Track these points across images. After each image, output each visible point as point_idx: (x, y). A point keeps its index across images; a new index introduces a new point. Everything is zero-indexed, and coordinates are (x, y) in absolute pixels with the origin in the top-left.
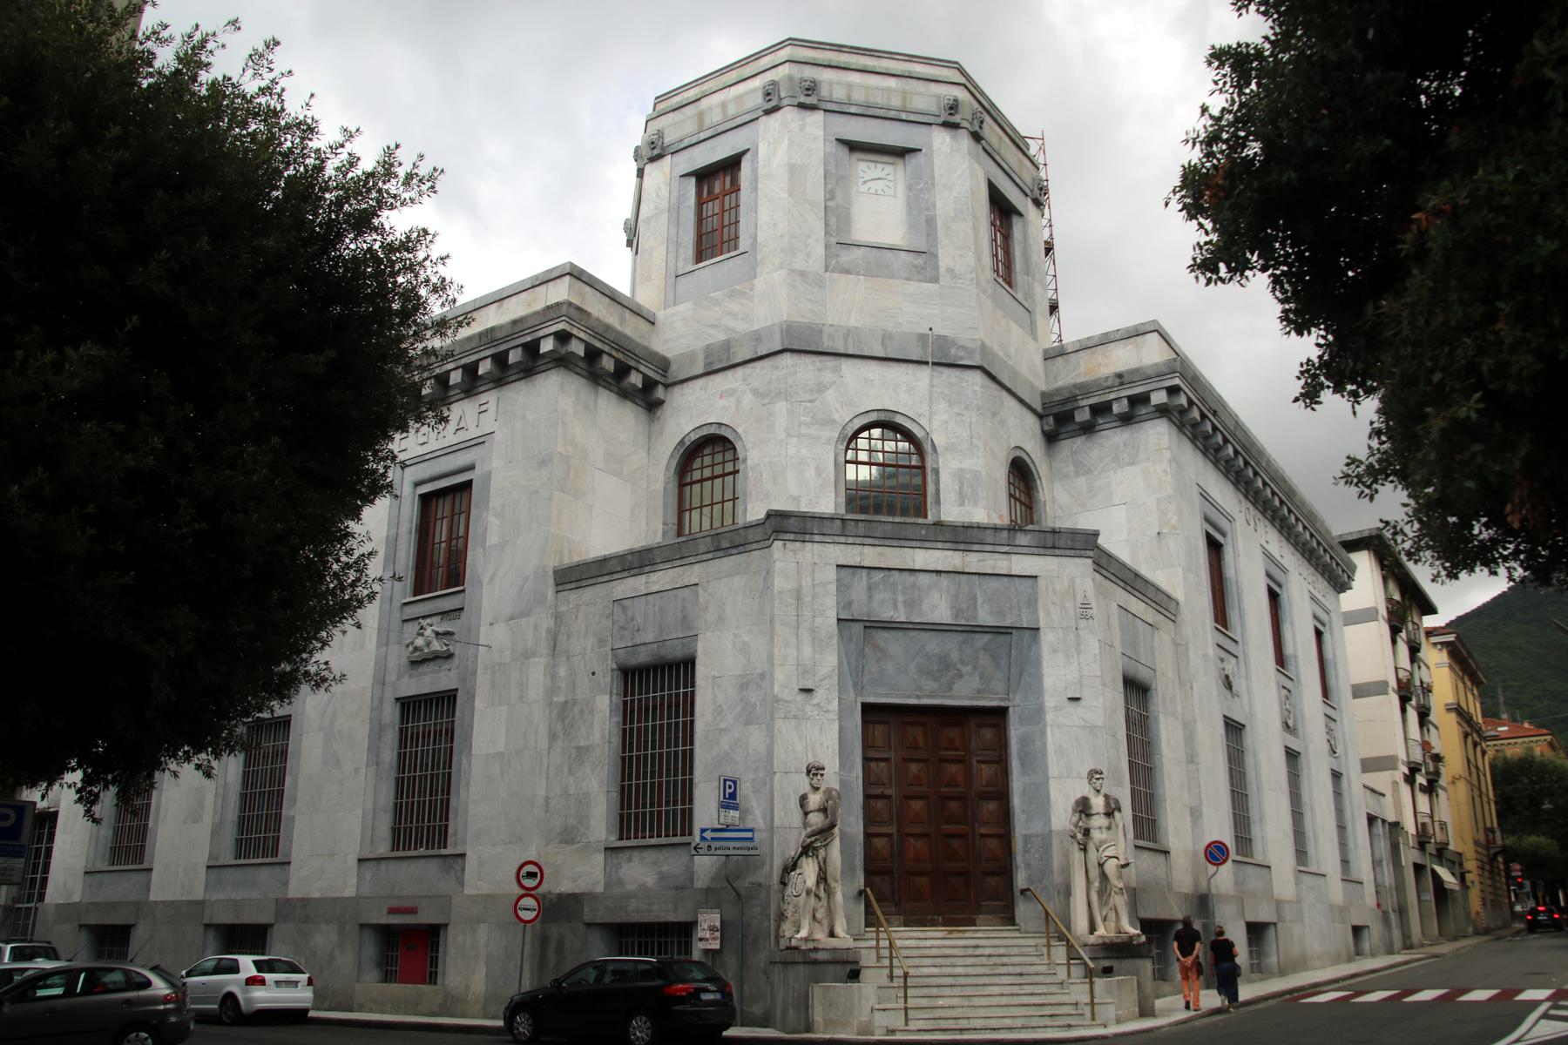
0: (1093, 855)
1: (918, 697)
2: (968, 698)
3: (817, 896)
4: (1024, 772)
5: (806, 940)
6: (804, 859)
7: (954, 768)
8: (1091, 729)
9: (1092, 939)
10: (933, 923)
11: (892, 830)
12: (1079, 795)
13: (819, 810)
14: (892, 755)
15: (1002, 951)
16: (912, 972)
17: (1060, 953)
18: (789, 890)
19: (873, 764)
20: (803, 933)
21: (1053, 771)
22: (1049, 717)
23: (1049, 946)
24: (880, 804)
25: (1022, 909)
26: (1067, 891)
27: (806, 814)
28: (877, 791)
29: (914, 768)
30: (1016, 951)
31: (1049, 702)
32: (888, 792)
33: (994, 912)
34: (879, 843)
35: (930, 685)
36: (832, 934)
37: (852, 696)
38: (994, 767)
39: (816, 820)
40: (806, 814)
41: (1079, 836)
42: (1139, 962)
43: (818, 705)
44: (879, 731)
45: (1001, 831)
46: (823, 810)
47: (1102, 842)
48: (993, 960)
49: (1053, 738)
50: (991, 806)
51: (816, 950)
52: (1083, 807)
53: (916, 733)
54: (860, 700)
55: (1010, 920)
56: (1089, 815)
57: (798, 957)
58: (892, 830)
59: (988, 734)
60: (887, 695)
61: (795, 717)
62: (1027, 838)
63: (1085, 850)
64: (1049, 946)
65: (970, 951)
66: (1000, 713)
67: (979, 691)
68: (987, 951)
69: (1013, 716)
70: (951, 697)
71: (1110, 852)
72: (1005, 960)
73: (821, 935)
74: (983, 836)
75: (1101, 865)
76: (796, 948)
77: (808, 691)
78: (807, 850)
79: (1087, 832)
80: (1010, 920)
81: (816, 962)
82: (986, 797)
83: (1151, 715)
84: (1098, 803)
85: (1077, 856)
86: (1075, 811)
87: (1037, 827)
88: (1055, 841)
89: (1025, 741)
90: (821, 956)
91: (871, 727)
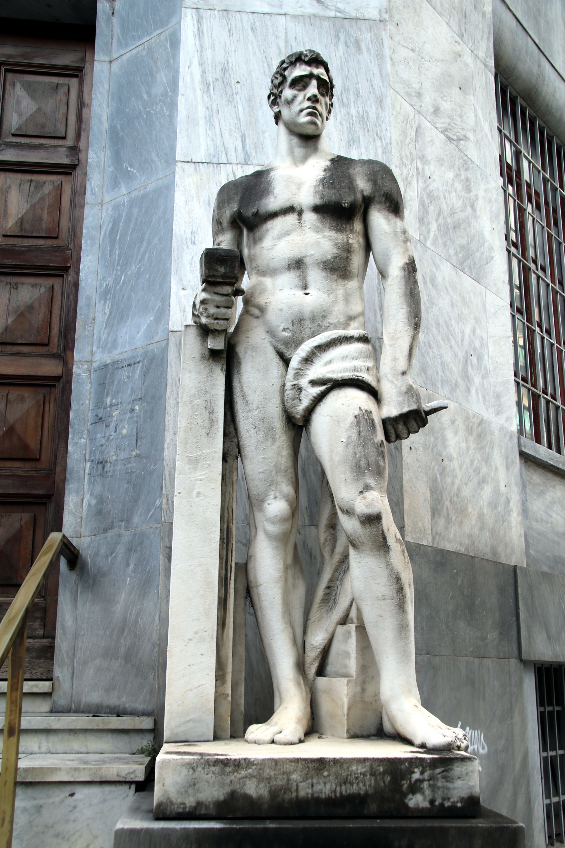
0: (259, 377)
4: (120, 174)
45: (50, 368)
47: (303, 325)
52: (246, 208)
62: (106, 375)
63: (227, 357)
75: (298, 426)
84: (298, 180)
85: (191, 384)
87: (133, 337)
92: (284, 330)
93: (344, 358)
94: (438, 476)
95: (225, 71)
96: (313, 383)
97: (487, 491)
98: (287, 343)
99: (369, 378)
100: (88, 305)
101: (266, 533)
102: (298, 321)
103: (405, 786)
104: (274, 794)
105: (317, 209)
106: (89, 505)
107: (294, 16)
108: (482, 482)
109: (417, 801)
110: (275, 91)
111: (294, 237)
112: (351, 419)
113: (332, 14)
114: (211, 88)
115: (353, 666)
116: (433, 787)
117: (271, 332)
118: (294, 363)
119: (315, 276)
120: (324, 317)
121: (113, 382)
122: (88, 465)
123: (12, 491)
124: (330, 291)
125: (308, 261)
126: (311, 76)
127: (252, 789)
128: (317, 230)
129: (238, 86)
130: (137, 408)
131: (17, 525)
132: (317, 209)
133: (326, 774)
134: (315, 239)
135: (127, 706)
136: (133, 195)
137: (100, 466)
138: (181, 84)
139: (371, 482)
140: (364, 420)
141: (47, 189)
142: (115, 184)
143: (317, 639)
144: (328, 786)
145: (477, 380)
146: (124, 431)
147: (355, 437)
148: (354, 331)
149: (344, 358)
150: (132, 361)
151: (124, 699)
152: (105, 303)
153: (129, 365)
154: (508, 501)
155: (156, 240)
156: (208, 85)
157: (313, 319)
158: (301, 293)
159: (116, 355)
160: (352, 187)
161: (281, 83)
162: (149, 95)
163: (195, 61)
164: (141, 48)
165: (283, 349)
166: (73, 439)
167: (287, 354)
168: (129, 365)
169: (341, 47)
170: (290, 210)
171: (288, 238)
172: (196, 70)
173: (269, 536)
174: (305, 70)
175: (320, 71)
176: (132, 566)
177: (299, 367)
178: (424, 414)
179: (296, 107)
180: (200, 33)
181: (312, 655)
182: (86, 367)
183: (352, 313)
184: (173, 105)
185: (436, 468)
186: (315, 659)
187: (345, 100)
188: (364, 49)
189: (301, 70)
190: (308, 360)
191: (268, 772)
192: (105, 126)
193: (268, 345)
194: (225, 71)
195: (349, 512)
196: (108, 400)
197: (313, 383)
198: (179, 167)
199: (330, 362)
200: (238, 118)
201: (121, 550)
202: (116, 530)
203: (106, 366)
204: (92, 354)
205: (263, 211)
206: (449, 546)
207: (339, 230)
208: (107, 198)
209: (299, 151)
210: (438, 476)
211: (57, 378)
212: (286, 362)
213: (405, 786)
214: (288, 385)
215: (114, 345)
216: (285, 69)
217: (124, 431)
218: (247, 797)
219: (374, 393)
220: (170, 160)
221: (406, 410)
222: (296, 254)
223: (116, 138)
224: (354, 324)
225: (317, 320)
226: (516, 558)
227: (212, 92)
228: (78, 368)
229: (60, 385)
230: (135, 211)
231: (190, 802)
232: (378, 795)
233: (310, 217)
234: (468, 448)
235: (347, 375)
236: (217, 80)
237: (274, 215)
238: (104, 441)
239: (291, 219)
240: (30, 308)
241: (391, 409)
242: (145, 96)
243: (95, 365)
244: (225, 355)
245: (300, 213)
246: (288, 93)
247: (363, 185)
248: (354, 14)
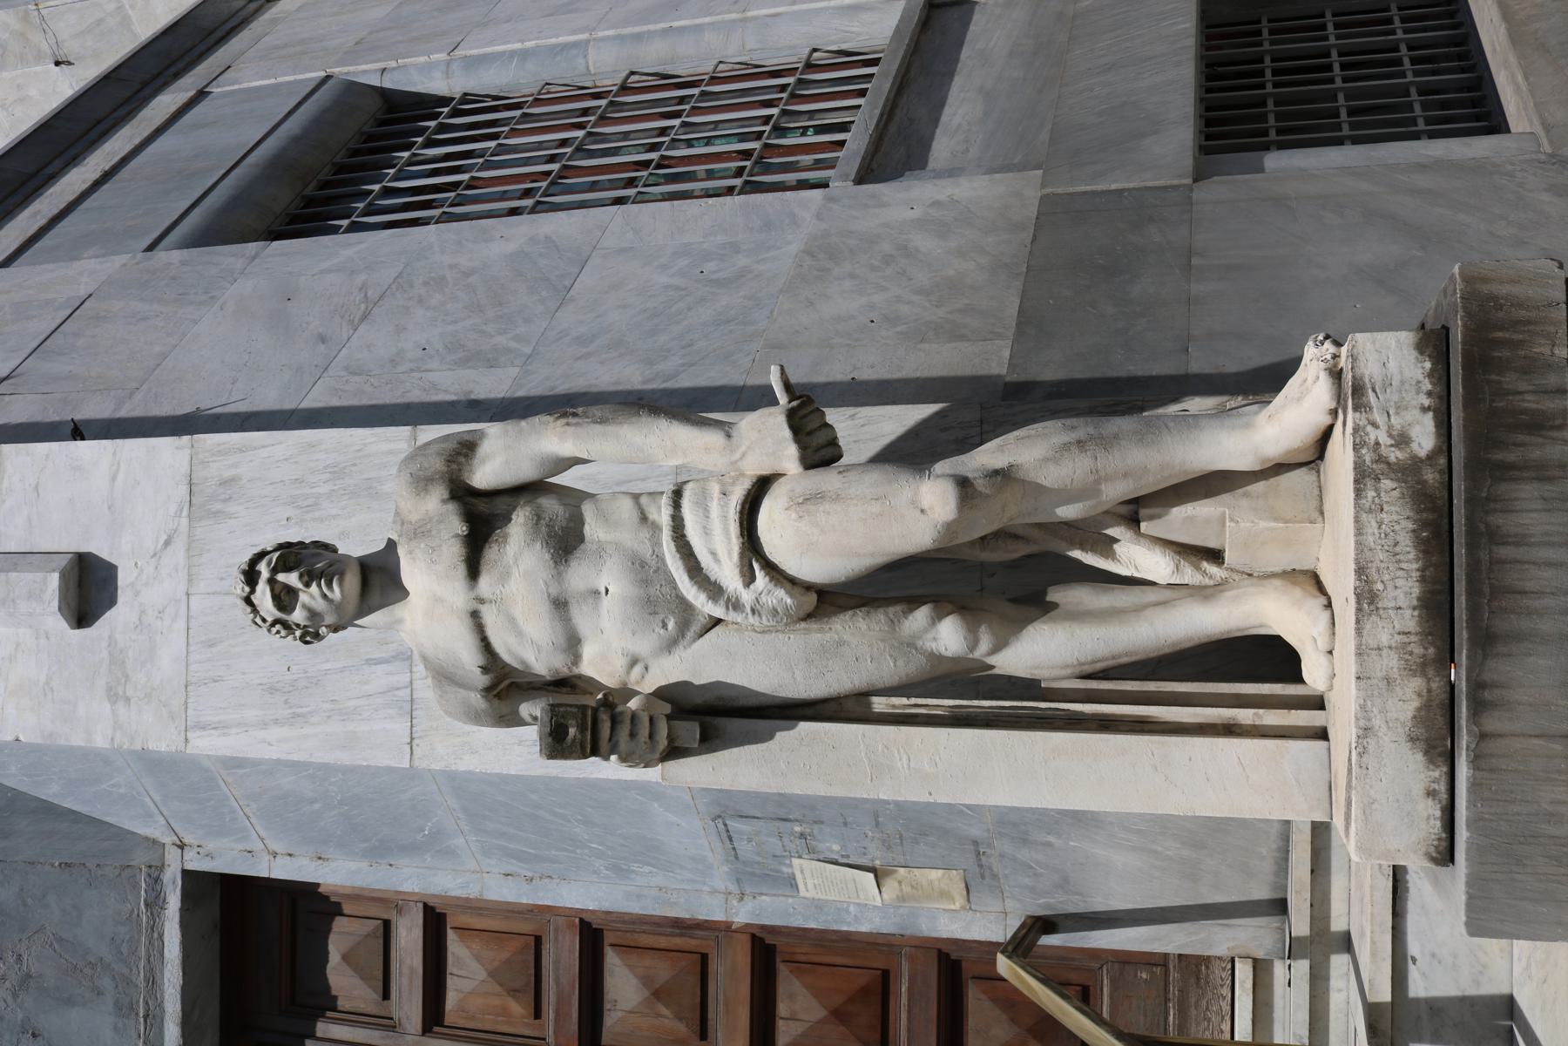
31: (96, 726)
67: (124, 1009)
71: (718, 548)
92: (664, 626)
93: (706, 531)
94: (899, 329)
95: (273, 690)
96: (749, 579)
97: (923, 242)
100: (639, 897)
103: (1400, 455)
107: (190, 581)
108: (905, 250)
109: (1424, 438)
110: (298, 633)
111: (518, 611)
113: (184, 521)
114: (299, 711)
116: (1399, 408)
118: (718, 612)
119: (579, 575)
120: (643, 564)
124: (600, 552)
125: (554, 591)
126: (272, 581)
128: (505, 576)
129: (294, 668)
133: (1379, 586)
135: (1274, 846)
136: (466, 828)
138: (295, 758)
142: (450, 853)
144: (1400, 582)
145: (742, 261)
146: (836, 847)
149: (706, 531)
151: (1264, 851)
152: (636, 873)
153: (730, 839)
154: (936, 204)
155: (533, 797)
156: (295, 716)
157: (645, 582)
158: (606, 602)
161: (286, 625)
162: (312, 801)
163: (262, 734)
165: (695, 628)
166: (849, 924)
168: (730, 839)
169: (231, 508)
170: (475, 615)
171: (521, 621)
172: (275, 733)
173: (997, 649)
174: (264, 593)
175: (263, 568)
176: (1051, 839)
177: (722, 602)
178: (795, 403)
180: (221, 727)
181: (1189, 575)
182: (735, 902)
183: (635, 516)
184: (327, 769)
185: (884, 333)
186: (1198, 568)
187: (309, 502)
188: (232, 472)
190: (714, 590)
193: (689, 651)
194: (273, 690)
197: (749, 579)
198: (420, 763)
199: (714, 554)
200: (342, 670)
201: (1024, 854)
204: (714, 891)
206: (1012, 309)
208: (472, 865)
210: (899, 329)
212: (718, 621)
213: (1400, 455)
216: (264, 620)
217: (836, 847)
219: (762, 485)
220: (411, 775)
222: (544, 608)
224: (653, 515)
226: (1027, 190)
227: (304, 710)
228: (737, 914)
234: (852, 276)
235: (734, 528)
236: (286, 702)
239: (490, 618)
240: (646, 981)
241: (788, 457)
242: (317, 806)
243: (733, 887)
244: (709, 719)
246: (298, 616)
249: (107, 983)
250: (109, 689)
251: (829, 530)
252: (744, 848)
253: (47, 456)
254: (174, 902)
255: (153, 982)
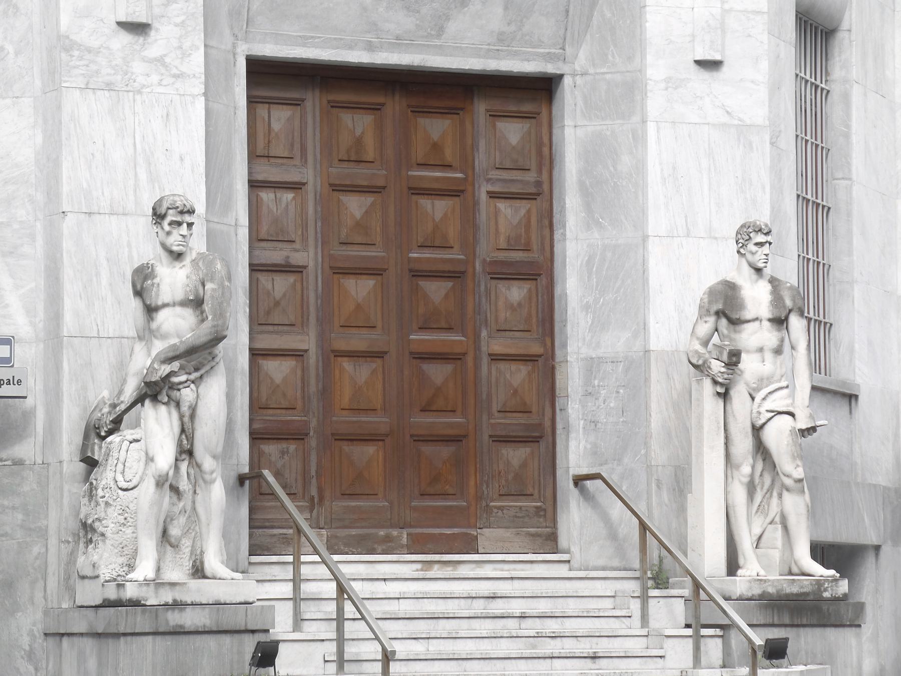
1: (370, 47)
2: (477, 53)
3: (175, 489)
4: (591, 221)
5: (157, 583)
6: (148, 409)
7: (438, 209)
8: (743, 130)
9: (740, 585)
10: (389, 546)
11: (308, 341)
12: (711, 280)
13: (184, 303)
14: (308, 174)
15: (543, 606)
16: (401, 649)
17: (669, 611)
18: (105, 477)
19: (267, 196)
20: (145, 569)
21: (657, 222)
22: (655, 104)
23: (644, 598)
24: (280, 285)
25: (574, 517)
26: (681, 482)
27: (151, 310)
28: (274, 255)
29: (355, 206)
30: (571, 607)
32: (298, 258)
33: (516, 522)
34: (277, 369)
35: (399, 21)
36: (199, 572)
37: (228, 39)
38: (523, 207)
39: (178, 326)
40: (151, 310)
41: (717, 367)
42: (831, 634)
43: (160, 60)
44: (280, 118)
46: (196, 303)
47: (763, 381)
48: (531, 627)
49: (661, 149)
50: (516, 292)
51: (177, 605)
53: (358, 124)
54: (243, 50)
55: (549, 541)
56: (735, 322)
57: (141, 622)
58: (308, 341)
59: (513, 132)
60: (304, 41)
61: (109, 87)
62: (592, 366)
63: (725, 396)
64: (644, 598)
65: (479, 607)
66: (541, 89)
67: (501, 38)
68: (517, 607)
69: (570, 96)
70: (440, 50)
71: (779, 402)
72: (553, 626)
73: (176, 573)
74: (496, 358)
75: (757, 430)
76: (135, 603)
77: (138, 28)
78: (154, 391)
79: (733, 359)
80: (549, 541)
81: (179, 632)
82: (504, 272)
83: (836, 89)
86: (704, 312)
88: (655, 374)
89: (597, 152)
90: (190, 619)
91: (262, 111)
98: (754, 389)
99: (791, 409)
100: (574, 314)
101: (740, 481)
102: (761, 380)
104: (778, 592)
105: (770, 320)
106: (585, 448)
107: (714, 125)
109: (826, 595)
112: (788, 432)
113: (736, 122)
115: (779, 543)
117: (747, 384)
118: (758, 399)
119: (769, 356)
121: (599, 371)
122: (582, 422)
123: (520, 434)
127: (771, 590)
130: (621, 391)
131: (524, 456)
132: (770, 320)
134: (767, 335)
137: (593, 424)
139: (799, 463)
140: (793, 430)
141: (523, 212)
142: (588, 228)
143: (757, 531)
147: (791, 441)
148: (784, 384)
149: (781, 398)
150: (615, 360)
152: (587, 314)
157: (768, 379)
158: (761, 365)
159: (600, 352)
160: (784, 306)
162: (616, 170)
164: (605, 127)
165: (752, 392)
167: (754, 395)
179: (757, 257)
189: (761, 238)
191: (775, 584)
192: (575, 179)
194: (674, 168)
195: (788, 476)
196: (596, 382)
202: (610, 465)
203: (592, 358)
204: (579, 348)
205: (743, 318)
207: (779, 330)
209: (754, 276)
211: (540, 356)
212: (753, 399)
214: (755, 411)
215: (598, 345)
218: (769, 593)
221: (809, 426)
222: (760, 345)
223: (585, 192)
224: (783, 379)
225: (769, 379)
229: (541, 360)
230: (609, 255)
231: (750, 595)
232: (814, 592)
233: (766, 324)
235: (785, 409)
237: (748, 321)
238: (594, 408)
239: (757, 323)
241: (803, 424)
242: (612, 169)
243: (582, 356)
245: (761, 321)
247: (789, 303)
248: (748, 122)
249: (513, 28)
250: (670, 78)
251: (778, 435)
252: (609, 367)
253: (762, 42)
254: (550, 69)
255: (515, 55)
